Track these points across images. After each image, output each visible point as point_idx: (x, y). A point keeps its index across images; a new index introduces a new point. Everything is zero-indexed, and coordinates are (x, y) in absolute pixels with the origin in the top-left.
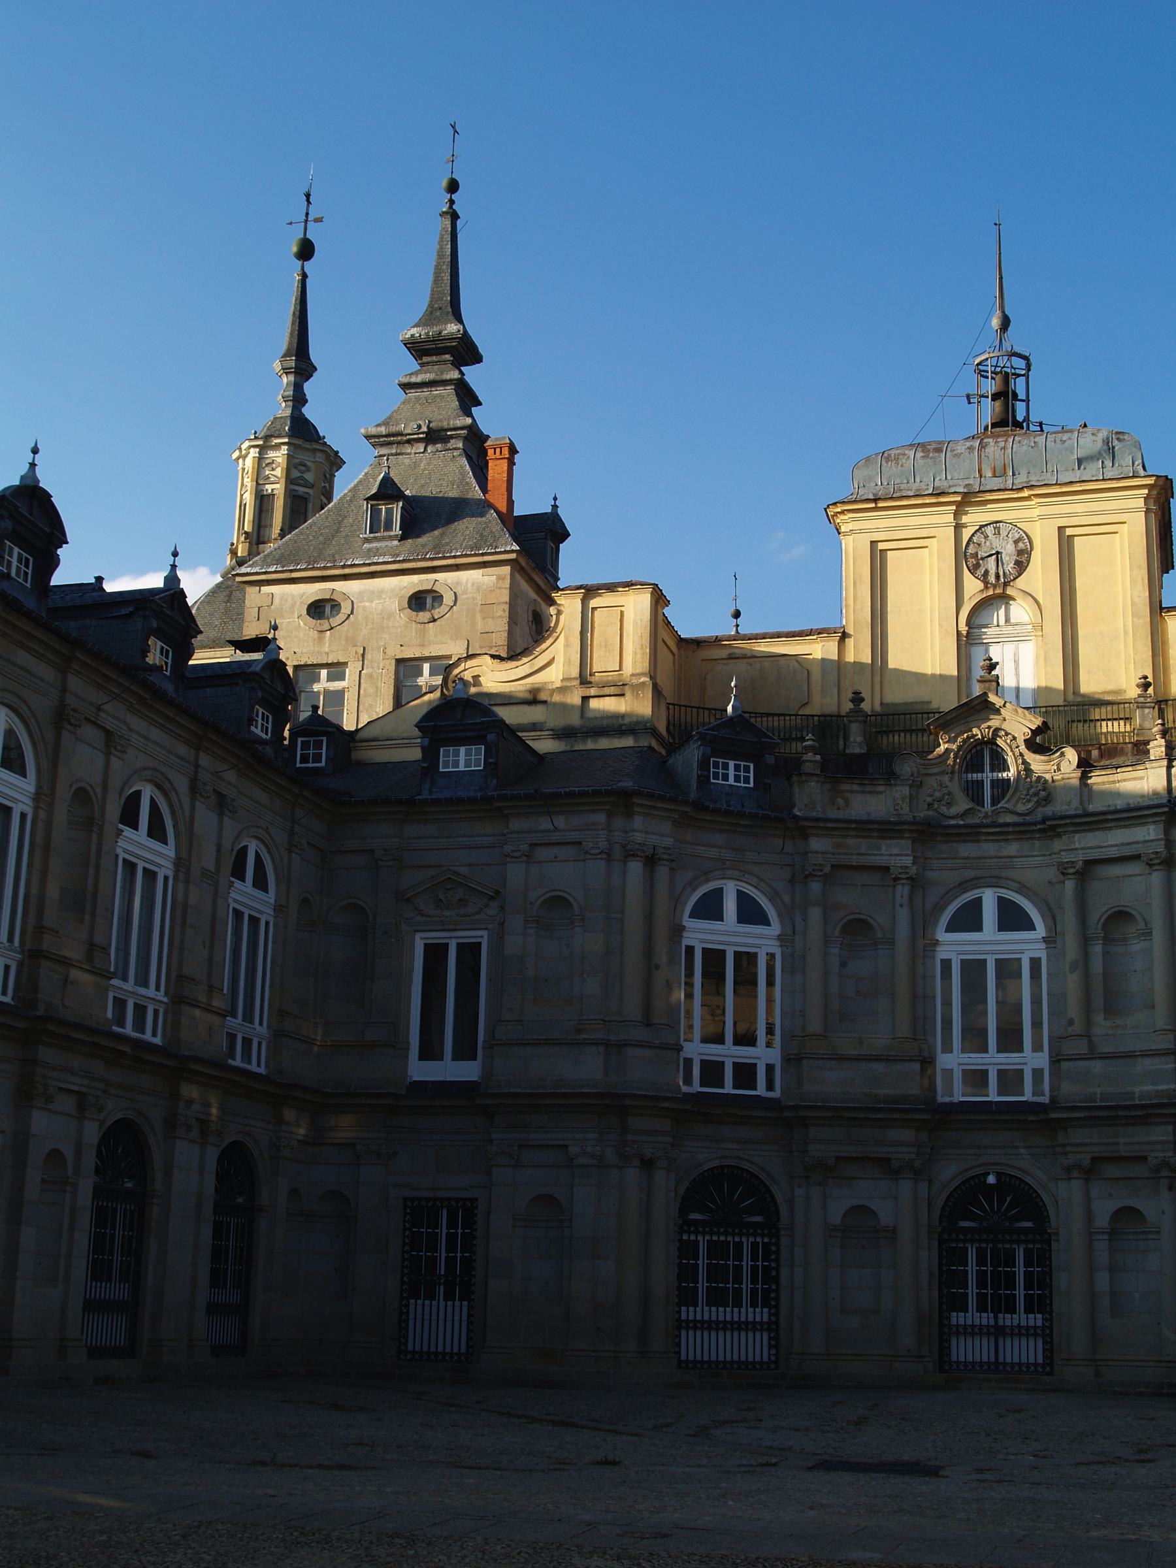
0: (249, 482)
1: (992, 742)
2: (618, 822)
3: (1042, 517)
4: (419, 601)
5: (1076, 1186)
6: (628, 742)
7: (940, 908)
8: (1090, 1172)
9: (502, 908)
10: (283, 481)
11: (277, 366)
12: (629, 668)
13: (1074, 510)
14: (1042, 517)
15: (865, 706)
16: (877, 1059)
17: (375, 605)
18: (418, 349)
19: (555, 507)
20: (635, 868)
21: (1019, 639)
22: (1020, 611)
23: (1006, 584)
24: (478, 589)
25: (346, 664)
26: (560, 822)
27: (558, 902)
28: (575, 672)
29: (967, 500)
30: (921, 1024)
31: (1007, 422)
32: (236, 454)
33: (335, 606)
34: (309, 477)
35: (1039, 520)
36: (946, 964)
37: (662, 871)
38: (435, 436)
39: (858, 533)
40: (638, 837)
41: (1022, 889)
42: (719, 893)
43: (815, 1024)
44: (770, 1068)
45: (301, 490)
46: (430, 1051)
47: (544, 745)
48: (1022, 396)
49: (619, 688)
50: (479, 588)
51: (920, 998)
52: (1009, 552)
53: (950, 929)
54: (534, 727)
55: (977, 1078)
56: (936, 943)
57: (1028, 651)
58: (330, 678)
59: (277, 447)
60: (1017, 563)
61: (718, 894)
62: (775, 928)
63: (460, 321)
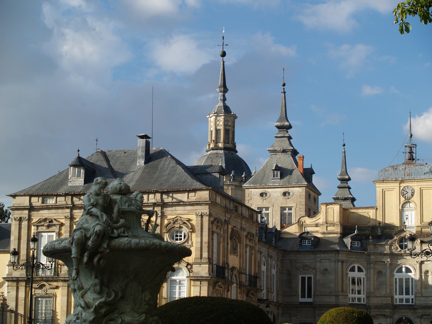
0: (212, 124)
1: (405, 237)
2: (337, 255)
3: (417, 186)
4: (285, 194)
5: (419, 320)
6: (336, 235)
7: (395, 269)
8: (421, 317)
9: (316, 271)
10: (223, 126)
11: (218, 90)
12: (335, 221)
13: (423, 184)
14: (417, 186)
15: (381, 225)
16: (383, 297)
17: (275, 195)
18: (278, 127)
19: (311, 167)
20: (340, 264)
21: (412, 210)
22: (412, 205)
23: (409, 199)
24: (298, 192)
25: (269, 207)
26: (326, 255)
27: (326, 270)
28: (325, 221)
29: (402, 181)
30: (391, 290)
31: (412, 159)
32: (208, 116)
33: (266, 194)
34: (230, 124)
35: (416, 186)
36: (396, 279)
37: (344, 264)
38: (284, 151)
39: (380, 187)
40: (340, 258)
41: (410, 265)
42: (354, 266)
43: (372, 291)
44: (364, 298)
45: (228, 128)
46: (303, 296)
47: (319, 236)
48: (415, 152)
49: (333, 224)
50: (299, 192)
51: (391, 285)
52: (410, 192)
53: (396, 272)
54: (317, 232)
55: (401, 300)
56: (394, 275)
57: (414, 213)
58: (265, 210)
59: (221, 116)
60: (412, 195)
61: (354, 267)
62: (364, 273)
63: (288, 121)
